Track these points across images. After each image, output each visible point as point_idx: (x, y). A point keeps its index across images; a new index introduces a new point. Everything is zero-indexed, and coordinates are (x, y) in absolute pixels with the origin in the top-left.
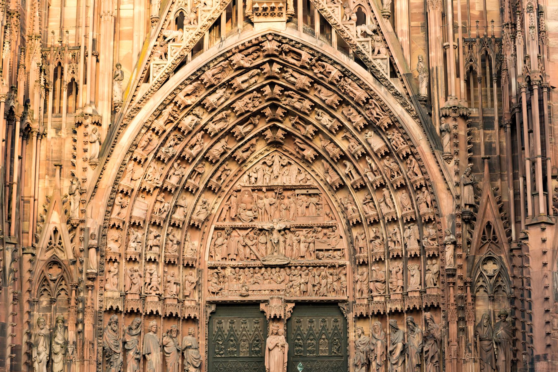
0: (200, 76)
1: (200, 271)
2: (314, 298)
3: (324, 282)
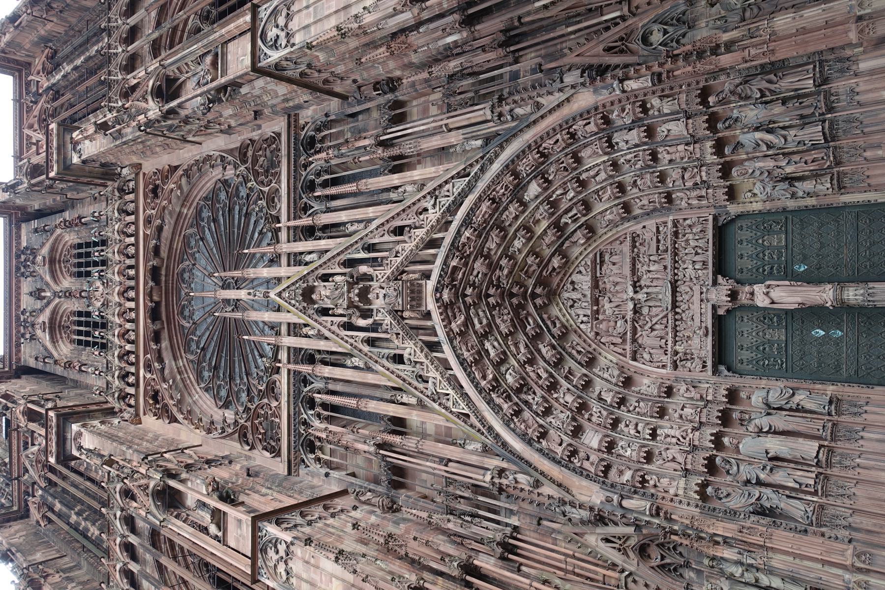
1: (677, 380)
2: (710, 253)
3: (693, 243)
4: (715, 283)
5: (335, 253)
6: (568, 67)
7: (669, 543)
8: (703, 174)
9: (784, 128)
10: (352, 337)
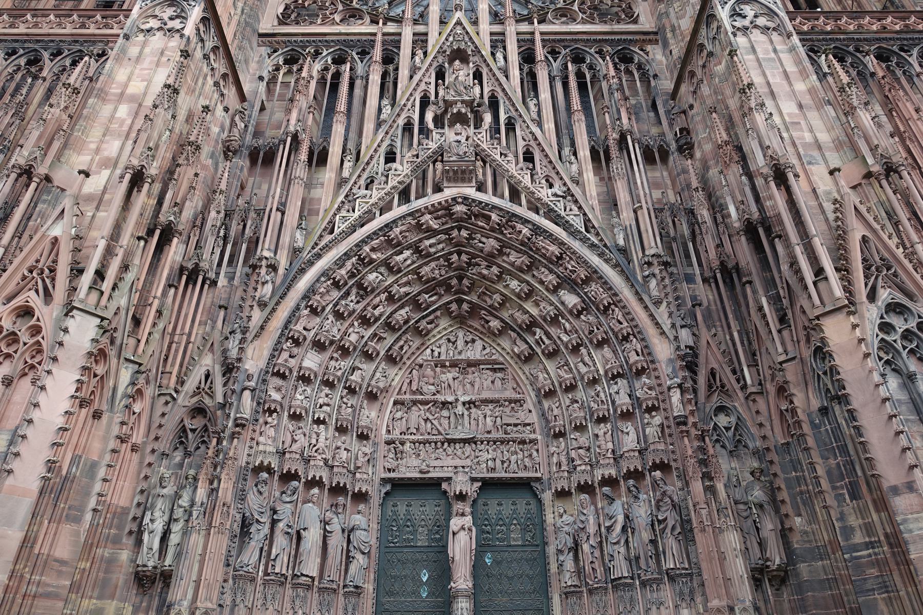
2: (503, 475)
3: (513, 458)
4: (473, 480)
5: (505, 86)
6: (697, 333)
7: (209, 437)
8: (583, 467)
9: (627, 542)
10: (413, 106)
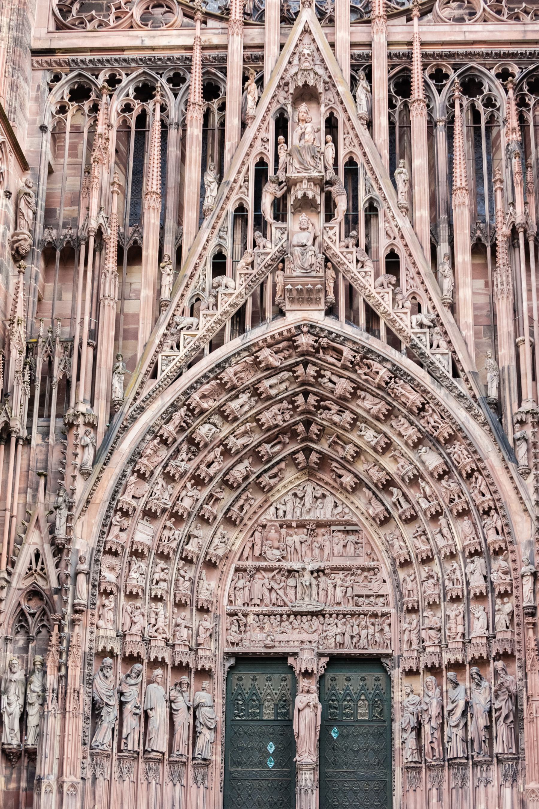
0: (219, 374)
5: (367, 150)
10: (246, 181)
